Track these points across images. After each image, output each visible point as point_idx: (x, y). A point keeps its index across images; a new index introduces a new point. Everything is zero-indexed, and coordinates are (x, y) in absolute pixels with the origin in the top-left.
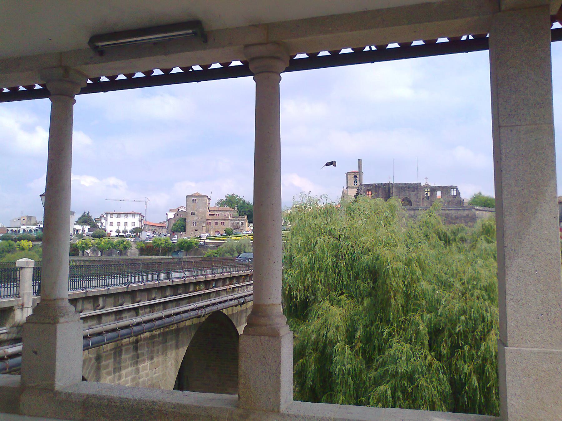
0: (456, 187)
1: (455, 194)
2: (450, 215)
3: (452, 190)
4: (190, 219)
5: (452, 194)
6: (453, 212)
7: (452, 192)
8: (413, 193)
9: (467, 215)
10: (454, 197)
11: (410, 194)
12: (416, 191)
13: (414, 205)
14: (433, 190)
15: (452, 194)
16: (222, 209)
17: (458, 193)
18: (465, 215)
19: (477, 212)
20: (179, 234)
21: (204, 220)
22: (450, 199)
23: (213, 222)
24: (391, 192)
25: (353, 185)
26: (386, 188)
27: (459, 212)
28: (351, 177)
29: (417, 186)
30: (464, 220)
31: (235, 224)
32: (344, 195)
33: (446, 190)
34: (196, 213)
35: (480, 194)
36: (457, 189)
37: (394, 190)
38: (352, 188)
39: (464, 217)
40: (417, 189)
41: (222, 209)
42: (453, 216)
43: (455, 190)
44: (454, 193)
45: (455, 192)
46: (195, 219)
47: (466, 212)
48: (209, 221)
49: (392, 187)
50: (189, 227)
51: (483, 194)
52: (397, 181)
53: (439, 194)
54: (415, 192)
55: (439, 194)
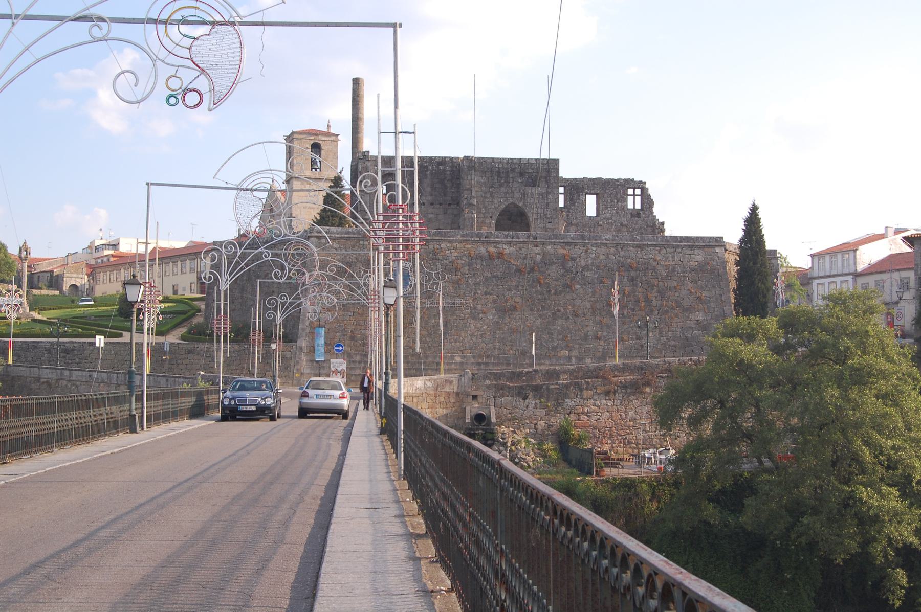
0: (642, 186)
1: (638, 206)
3: (630, 191)
7: (630, 199)
10: (636, 214)
12: (543, 184)
14: (577, 188)
15: (630, 206)
18: (693, 264)
24: (465, 183)
28: (303, 148)
29: (548, 171)
33: (611, 190)
36: (644, 191)
37: (474, 179)
39: (693, 270)
43: (638, 191)
44: (634, 202)
45: (638, 199)
53: (591, 202)
55: (591, 202)
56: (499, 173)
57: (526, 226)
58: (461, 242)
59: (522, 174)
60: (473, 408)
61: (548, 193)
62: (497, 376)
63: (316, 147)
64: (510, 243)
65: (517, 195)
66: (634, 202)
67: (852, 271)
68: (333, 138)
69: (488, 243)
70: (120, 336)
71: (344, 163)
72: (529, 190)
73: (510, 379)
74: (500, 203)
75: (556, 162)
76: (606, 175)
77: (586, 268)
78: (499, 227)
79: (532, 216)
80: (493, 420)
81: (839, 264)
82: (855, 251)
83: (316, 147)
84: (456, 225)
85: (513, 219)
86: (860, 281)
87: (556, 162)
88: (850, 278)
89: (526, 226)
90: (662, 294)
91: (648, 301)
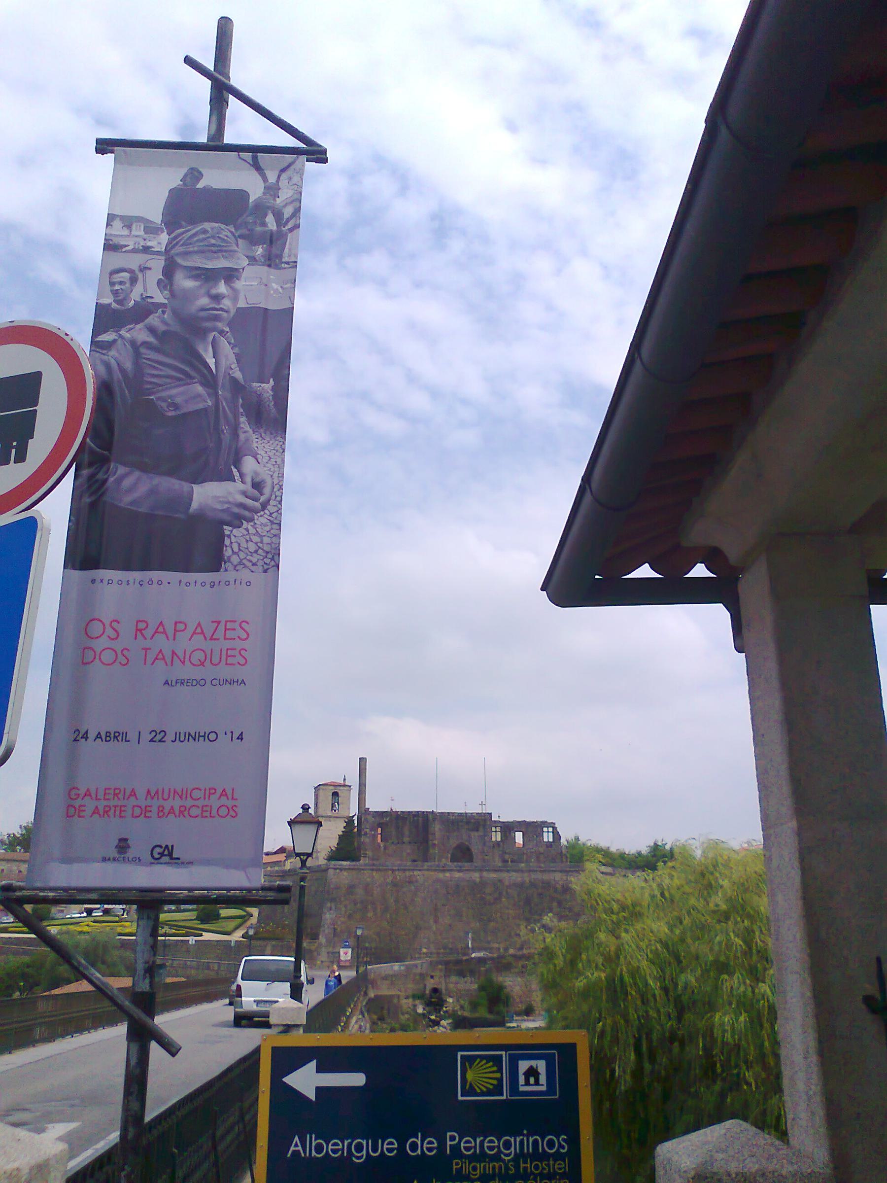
0: (553, 825)
1: (551, 840)
3: (545, 829)
5: (546, 840)
7: (545, 834)
8: (476, 834)
10: (549, 845)
11: (469, 836)
12: (481, 829)
13: (478, 863)
14: (508, 828)
15: (546, 840)
16: (11, 855)
17: (557, 836)
22: (541, 850)
25: (330, 814)
29: (485, 820)
33: (533, 829)
35: (577, 839)
36: (554, 828)
37: (437, 828)
40: (484, 826)
41: (11, 855)
42: (558, 886)
43: (551, 829)
44: (548, 837)
45: (551, 834)
49: (434, 819)
51: (582, 839)
53: (519, 837)
54: (481, 833)
55: (519, 837)
56: (453, 822)
58: (428, 870)
60: (430, 984)
61: (485, 836)
62: (447, 963)
63: (335, 794)
64: (459, 871)
66: (548, 837)
68: (347, 788)
69: (444, 871)
70: (201, 935)
71: (354, 810)
72: (474, 834)
74: (453, 842)
75: (490, 814)
77: (509, 887)
80: (444, 991)
83: (335, 794)
84: (426, 860)
85: (463, 854)
87: (490, 814)
90: (560, 904)
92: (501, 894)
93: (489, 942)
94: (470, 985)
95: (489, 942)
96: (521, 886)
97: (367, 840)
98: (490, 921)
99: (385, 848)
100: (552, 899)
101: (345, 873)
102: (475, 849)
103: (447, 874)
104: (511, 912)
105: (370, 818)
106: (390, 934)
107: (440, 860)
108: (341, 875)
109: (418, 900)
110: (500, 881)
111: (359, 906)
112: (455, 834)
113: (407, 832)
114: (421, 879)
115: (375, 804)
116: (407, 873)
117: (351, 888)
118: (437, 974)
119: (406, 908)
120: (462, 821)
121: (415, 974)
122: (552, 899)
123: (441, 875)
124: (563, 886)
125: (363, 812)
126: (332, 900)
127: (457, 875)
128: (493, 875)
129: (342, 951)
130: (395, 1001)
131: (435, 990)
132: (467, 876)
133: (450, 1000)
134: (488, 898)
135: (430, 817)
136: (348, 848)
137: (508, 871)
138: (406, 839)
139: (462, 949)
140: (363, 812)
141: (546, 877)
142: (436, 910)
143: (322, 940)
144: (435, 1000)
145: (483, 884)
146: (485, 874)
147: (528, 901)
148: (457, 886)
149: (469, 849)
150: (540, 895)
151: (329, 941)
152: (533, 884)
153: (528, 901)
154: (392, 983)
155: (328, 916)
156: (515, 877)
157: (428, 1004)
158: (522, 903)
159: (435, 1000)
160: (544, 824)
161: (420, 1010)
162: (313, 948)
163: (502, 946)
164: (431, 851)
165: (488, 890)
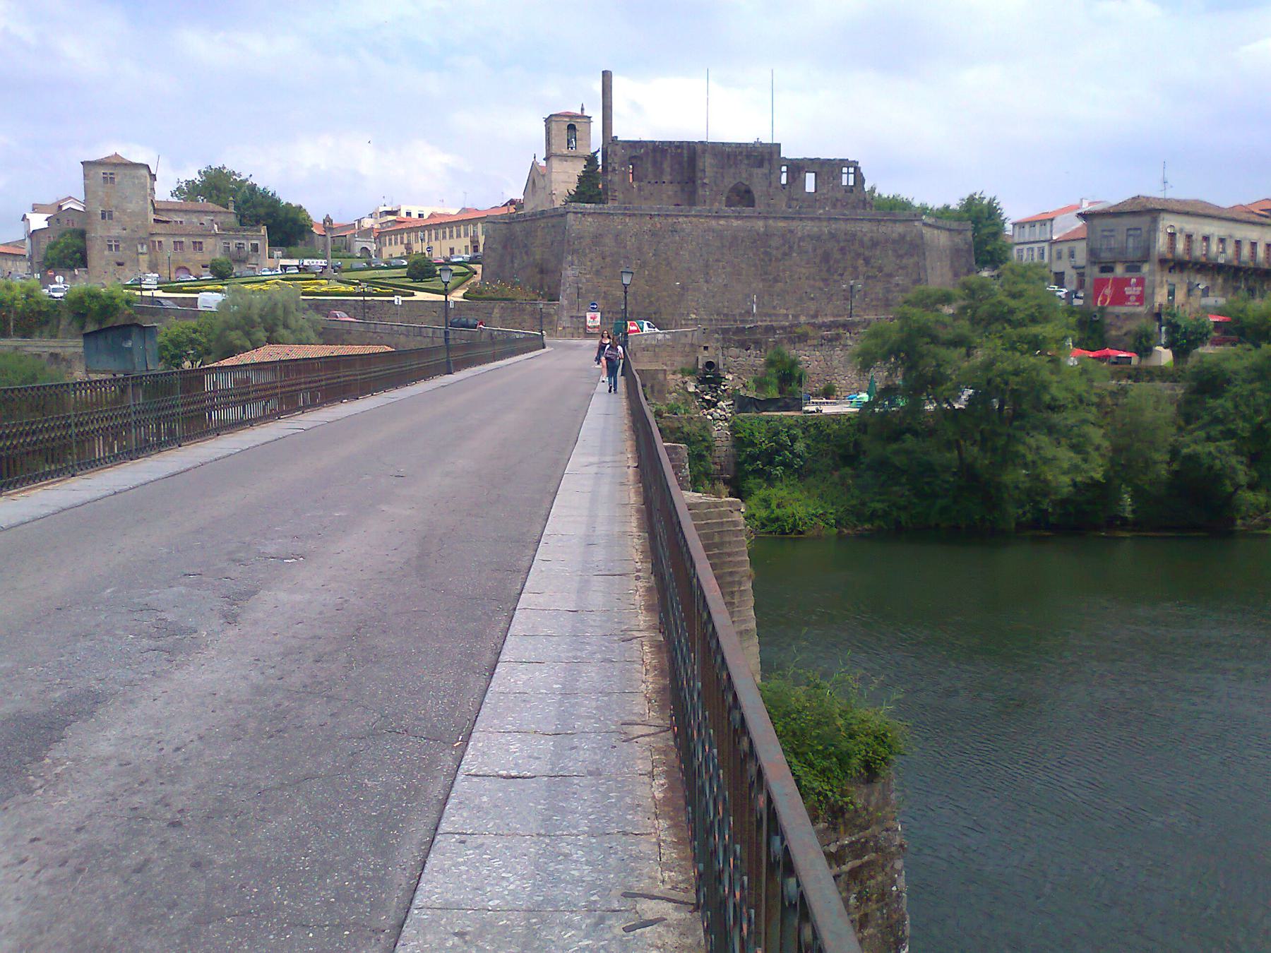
0: (855, 165)
1: (851, 183)
2: (859, 234)
3: (845, 170)
4: (99, 232)
5: (844, 183)
6: (866, 227)
7: (845, 176)
9: (902, 237)
10: (849, 189)
11: (751, 175)
12: (766, 164)
13: (760, 207)
14: (798, 168)
15: (844, 183)
16: (190, 205)
18: (895, 236)
19: (925, 230)
20: (68, 273)
21: (143, 234)
22: (839, 195)
23: (168, 242)
24: (700, 165)
25: (565, 152)
26: (681, 154)
27: (882, 229)
29: (771, 154)
30: (895, 251)
31: (232, 247)
32: (536, 179)
33: (828, 169)
34: (116, 214)
37: (707, 164)
38: (564, 157)
39: (894, 242)
40: (770, 160)
41: (190, 205)
42: (865, 239)
43: (851, 170)
44: (847, 180)
45: (852, 176)
46: (116, 231)
47: (900, 228)
48: (157, 239)
49: (704, 152)
50: (98, 255)
52: (712, 139)
53: (810, 179)
54: (765, 170)
55: (810, 179)
56: (729, 156)
57: (751, 203)
58: (695, 216)
59: (748, 156)
60: (704, 356)
62: (725, 331)
63: (571, 128)
64: (736, 218)
65: (744, 175)
66: (847, 180)
67: (1048, 237)
69: (719, 217)
70: (413, 295)
71: (596, 141)
72: (756, 171)
73: (734, 334)
74: (729, 182)
75: (779, 145)
76: (824, 156)
77: (801, 239)
78: (729, 203)
79: (757, 193)
80: (721, 366)
81: (1038, 233)
82: (1052, 220)
83: (571, 128)
84: (692, 203)
85: (743, 196)
86: (1055, 248)
87: (779, 145)
88: (1046, 245)
89: (751, 203)
90: (867, 261)
91: (855, 268)
92: (790, 248)
93: (774, 308)
94: (756, 359)
95: (774, 308)
96: (818, 238)
97: (616, 179)
98: (776, 280)
99: (640, 189)
100: (858, 255)
101: (590, 219)
102: (758, 190)
103: (722, 222)
104: (803, 270)
105: (618, 148)
106: (649, 296)
107: (712, 204)
108: (583, 223)
109: (685, 254)
110: (791, 232)
111: (608, 260)
112: (732, 170)
113: (668, 170)
114: (688, 228)
115: (625, 130)
116: (670, 220)
117: (597, 239)
118: (712, 344)
119: (668, 264)
120: (741, 153)
121: (684, 345)
122: (858, 255)
123: (714, 222)
124: (872, 239)
125: (609, 141)
126: (575, 252)
127: (735, 223)
128: (781, 224)
129: (589, 315)
130: (661, 376)
131: (710, 365)
132: (748, 224)
133: (730, 377)
134: (774, 252)
135: (699, 148)
136: (591, 187)
137: (801, 219)
138: (667, 178)
139: (741, 314)
140: (609, 141)
141: (851, 227)
142: (707, 266)
143: (563, 301)
144: (710, 377)
145: (768, 235)
146: (771, 222)
147: (826, 257)
148: (735, 238)
149: (748, 192)
150: (842, 250)
151: (571, 303)
152: (833, 236)
153: (826, 257)
154: (656, 355)
155: (569, 273)
156: (810, 227)
157: (703, 381)
158: (817, 260)
159: (710, 377)
160: (844, 163)
161: (691, 389)
162: (552, 311)
163: (791, 312)
164: (700, 192)
165: (775, 242)
